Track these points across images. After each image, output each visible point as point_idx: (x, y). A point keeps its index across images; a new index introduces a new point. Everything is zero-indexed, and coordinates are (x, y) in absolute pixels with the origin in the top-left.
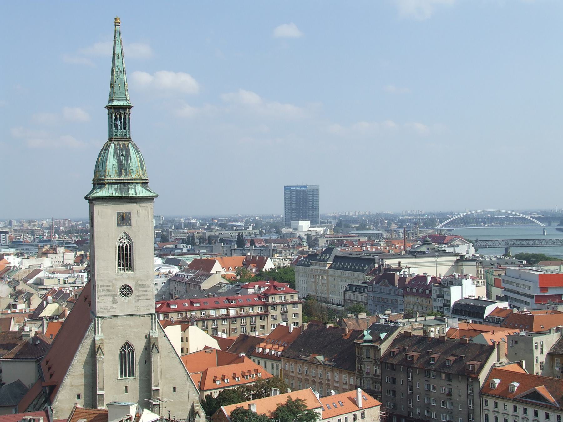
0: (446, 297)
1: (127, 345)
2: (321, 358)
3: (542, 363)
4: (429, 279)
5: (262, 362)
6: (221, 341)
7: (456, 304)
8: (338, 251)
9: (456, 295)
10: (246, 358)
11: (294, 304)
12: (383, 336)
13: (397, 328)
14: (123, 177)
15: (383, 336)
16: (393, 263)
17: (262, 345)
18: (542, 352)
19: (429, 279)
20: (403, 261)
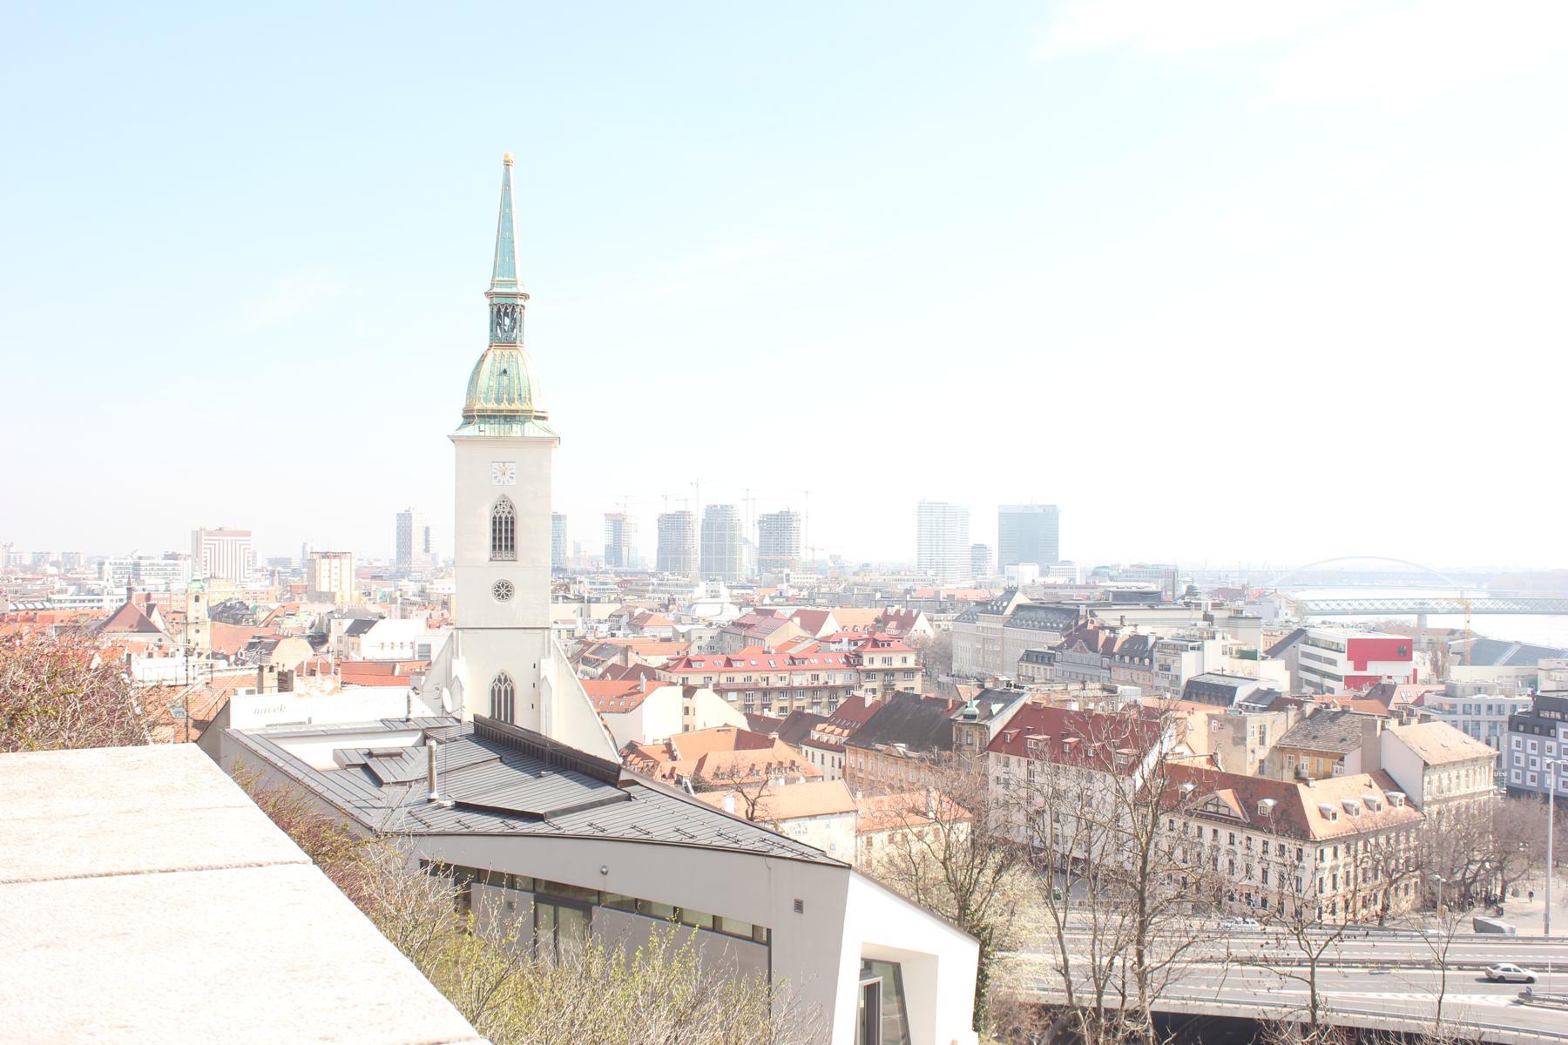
0: (1173, 671)
1: (503, 679)
2: (901, 748)
3: (1262, 762)
4: (1151, 641)
5: (818, 753)
6: (751, 718)
7: (1190, 683)
8: (1020, 599)
9: (1189, 667)
10: (778, 743)
11: (909, 672)
12: (995, 708)
13: (1020, 695)
14: (505, 406)
15: (995, 708)
16: (1108, 617)
17: (820, 727)
18: (1262, 742)
19: (1151, 641)
20: (1128, 615)
